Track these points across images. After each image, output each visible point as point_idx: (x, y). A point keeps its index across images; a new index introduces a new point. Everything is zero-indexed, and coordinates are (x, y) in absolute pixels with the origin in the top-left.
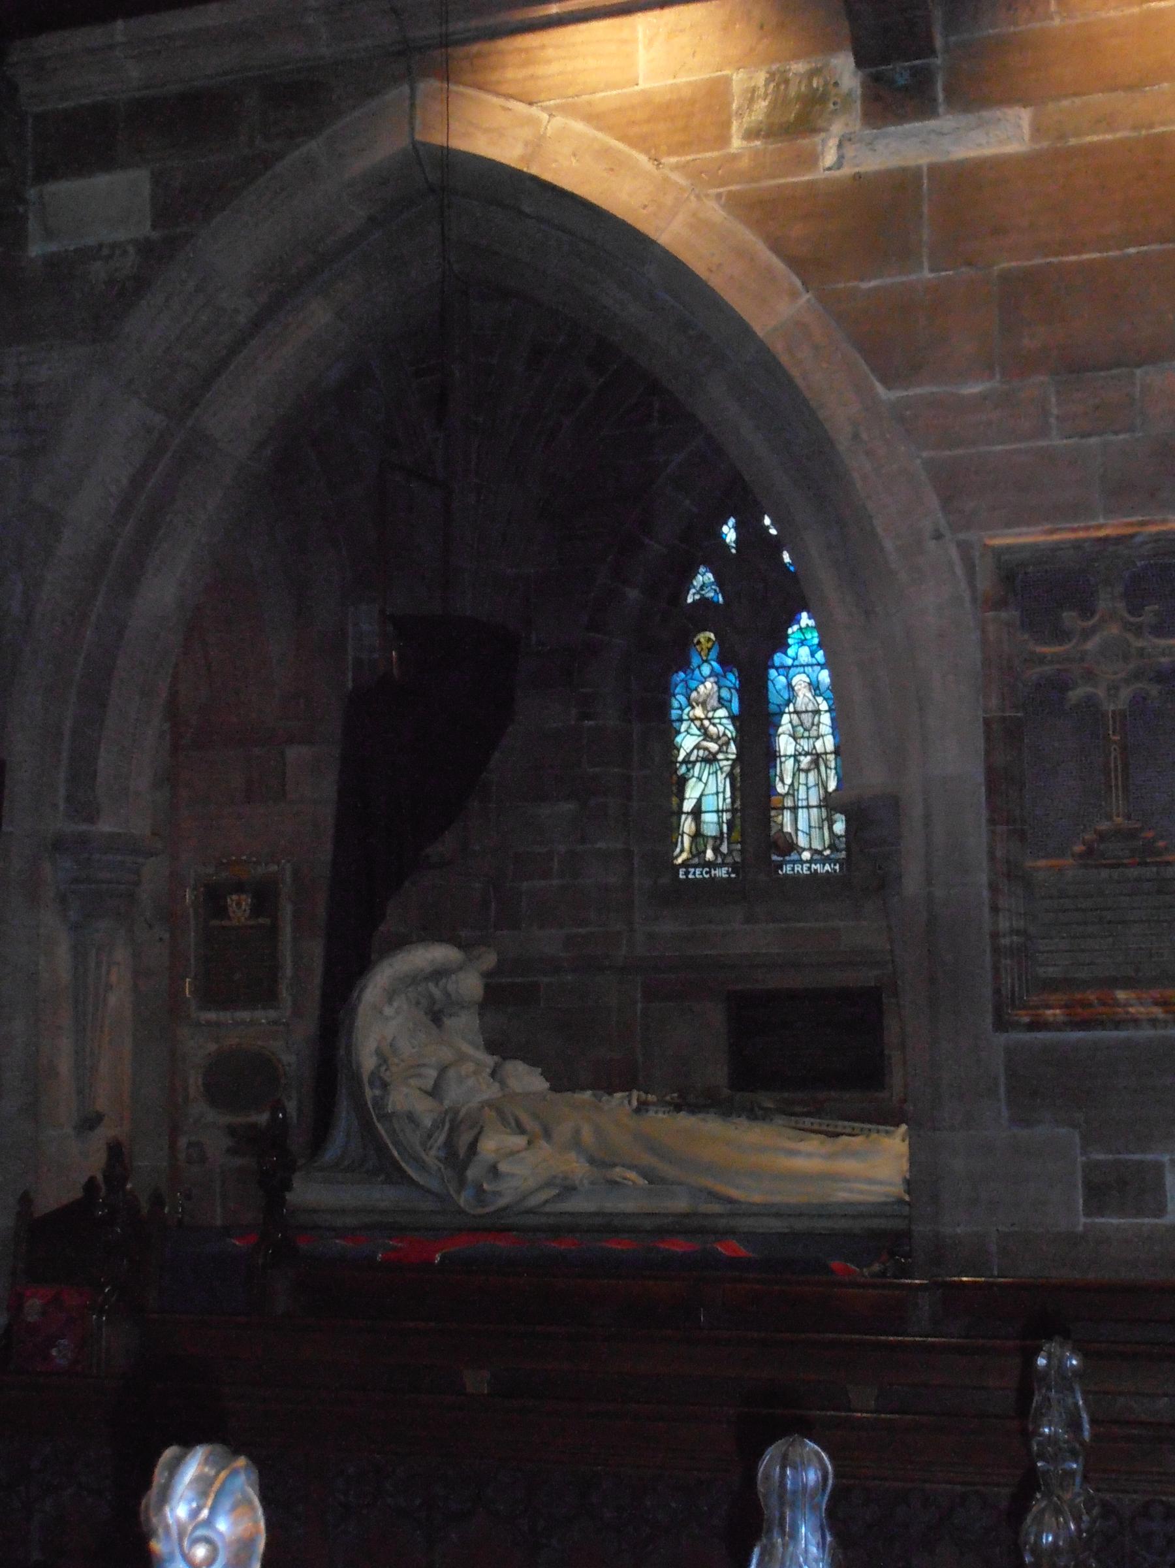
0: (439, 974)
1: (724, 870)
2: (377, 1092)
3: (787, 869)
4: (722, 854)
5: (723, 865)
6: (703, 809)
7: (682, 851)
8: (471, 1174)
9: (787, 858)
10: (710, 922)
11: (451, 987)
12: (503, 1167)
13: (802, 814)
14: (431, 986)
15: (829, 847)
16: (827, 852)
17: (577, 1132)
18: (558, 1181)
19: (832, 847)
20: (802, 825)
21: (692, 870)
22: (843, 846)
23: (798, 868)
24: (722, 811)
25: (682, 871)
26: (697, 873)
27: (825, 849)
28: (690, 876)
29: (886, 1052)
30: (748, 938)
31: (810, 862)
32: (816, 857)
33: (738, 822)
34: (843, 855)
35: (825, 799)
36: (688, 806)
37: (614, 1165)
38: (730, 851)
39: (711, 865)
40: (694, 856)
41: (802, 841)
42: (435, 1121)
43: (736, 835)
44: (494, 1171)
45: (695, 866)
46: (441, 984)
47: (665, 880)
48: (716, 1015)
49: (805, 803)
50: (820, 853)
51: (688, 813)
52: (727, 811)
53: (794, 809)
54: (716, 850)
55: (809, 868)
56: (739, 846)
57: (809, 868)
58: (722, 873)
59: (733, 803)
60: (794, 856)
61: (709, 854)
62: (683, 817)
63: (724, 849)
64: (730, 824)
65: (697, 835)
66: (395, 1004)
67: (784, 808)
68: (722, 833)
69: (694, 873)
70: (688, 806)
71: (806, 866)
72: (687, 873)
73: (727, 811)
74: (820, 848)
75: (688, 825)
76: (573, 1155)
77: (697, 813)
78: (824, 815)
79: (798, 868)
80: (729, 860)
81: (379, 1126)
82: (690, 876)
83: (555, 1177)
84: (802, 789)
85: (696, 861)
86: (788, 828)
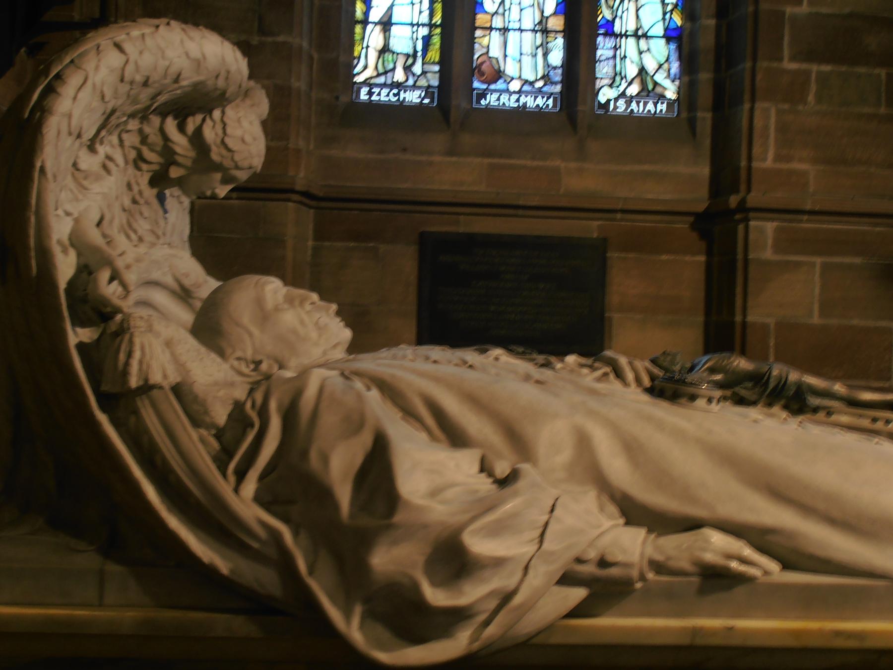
0: (193, 102)
1: (417, 93)
2: (86, 335)
3: (491, 100)
4: (414, 75)
5: (414, 87)
6: (393, 21)
7: (365, 67)
8: (383, 560)
9: (493, 87)
10: (405, 150)
11: (209, 134)
12: (478, 545)
13: (512, 36)
14: (171, 125)
15: (543, 78)
16: (539, 84)
17: (583, 442)
18: (588, 569)
19: (546, 77)
20: (512, 50)
21: (376, 90)
22: (558, 78)
23: (504, 98)
24: (418, 25)
25: (364, 91)
26: (384, 96)
27: (537, 80)
28: (374, 98)
29: (607, 315)
30: (452, 173)
31: (520, 92)
32: (526, 88)
33: (436, 40)
34: (558, 88)
35: (540, 23)
36: (376, 15)
37: (692, 525)
38: (424, 73)
39: (398, 85)
40: (379, 75)
41: (511, 69)
42: (238, 406)
43: (434, 54)
44: (452, 559)
45: (383, 86)
46: (191, 125)
47: (344, 99)
48: (405, 262)
49: (517, 26)
50: (532, 84)
51: (376, 24)
52: (423, 25)
53: (505, 30)
54: (407, 69)
55: (518, 100)
56: (437, 68)
57: (518, 100)
58: (413, 97)
59: (431, 16)
60: (500, 85)
61: (399, 75)
62: (370, 27)
63: (417, 69)
64: (427, 40)
65: (385, 50)
66: (102, 150)
67: (491, 29)
68: (415, 52)
69: (379, 94)
70: (376, 15)
71: (514, 97)
72: (370, 93)
73: (423, 25)
74: (532, 79)
75: (374, 38)
76: (590, 498)
77: (386, 24)
78: (539, 42)
79: (504, 98)
80: (422, 82)
81: (102, 418)
82: (374, 98)
83: (579, 560)
84: (515, 10)
85: (381, 80)
86: (495, 52)
